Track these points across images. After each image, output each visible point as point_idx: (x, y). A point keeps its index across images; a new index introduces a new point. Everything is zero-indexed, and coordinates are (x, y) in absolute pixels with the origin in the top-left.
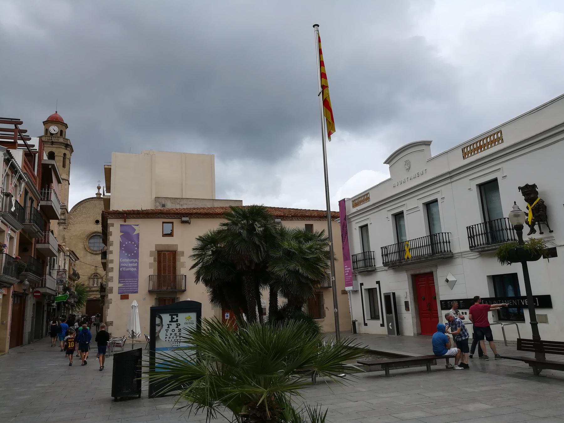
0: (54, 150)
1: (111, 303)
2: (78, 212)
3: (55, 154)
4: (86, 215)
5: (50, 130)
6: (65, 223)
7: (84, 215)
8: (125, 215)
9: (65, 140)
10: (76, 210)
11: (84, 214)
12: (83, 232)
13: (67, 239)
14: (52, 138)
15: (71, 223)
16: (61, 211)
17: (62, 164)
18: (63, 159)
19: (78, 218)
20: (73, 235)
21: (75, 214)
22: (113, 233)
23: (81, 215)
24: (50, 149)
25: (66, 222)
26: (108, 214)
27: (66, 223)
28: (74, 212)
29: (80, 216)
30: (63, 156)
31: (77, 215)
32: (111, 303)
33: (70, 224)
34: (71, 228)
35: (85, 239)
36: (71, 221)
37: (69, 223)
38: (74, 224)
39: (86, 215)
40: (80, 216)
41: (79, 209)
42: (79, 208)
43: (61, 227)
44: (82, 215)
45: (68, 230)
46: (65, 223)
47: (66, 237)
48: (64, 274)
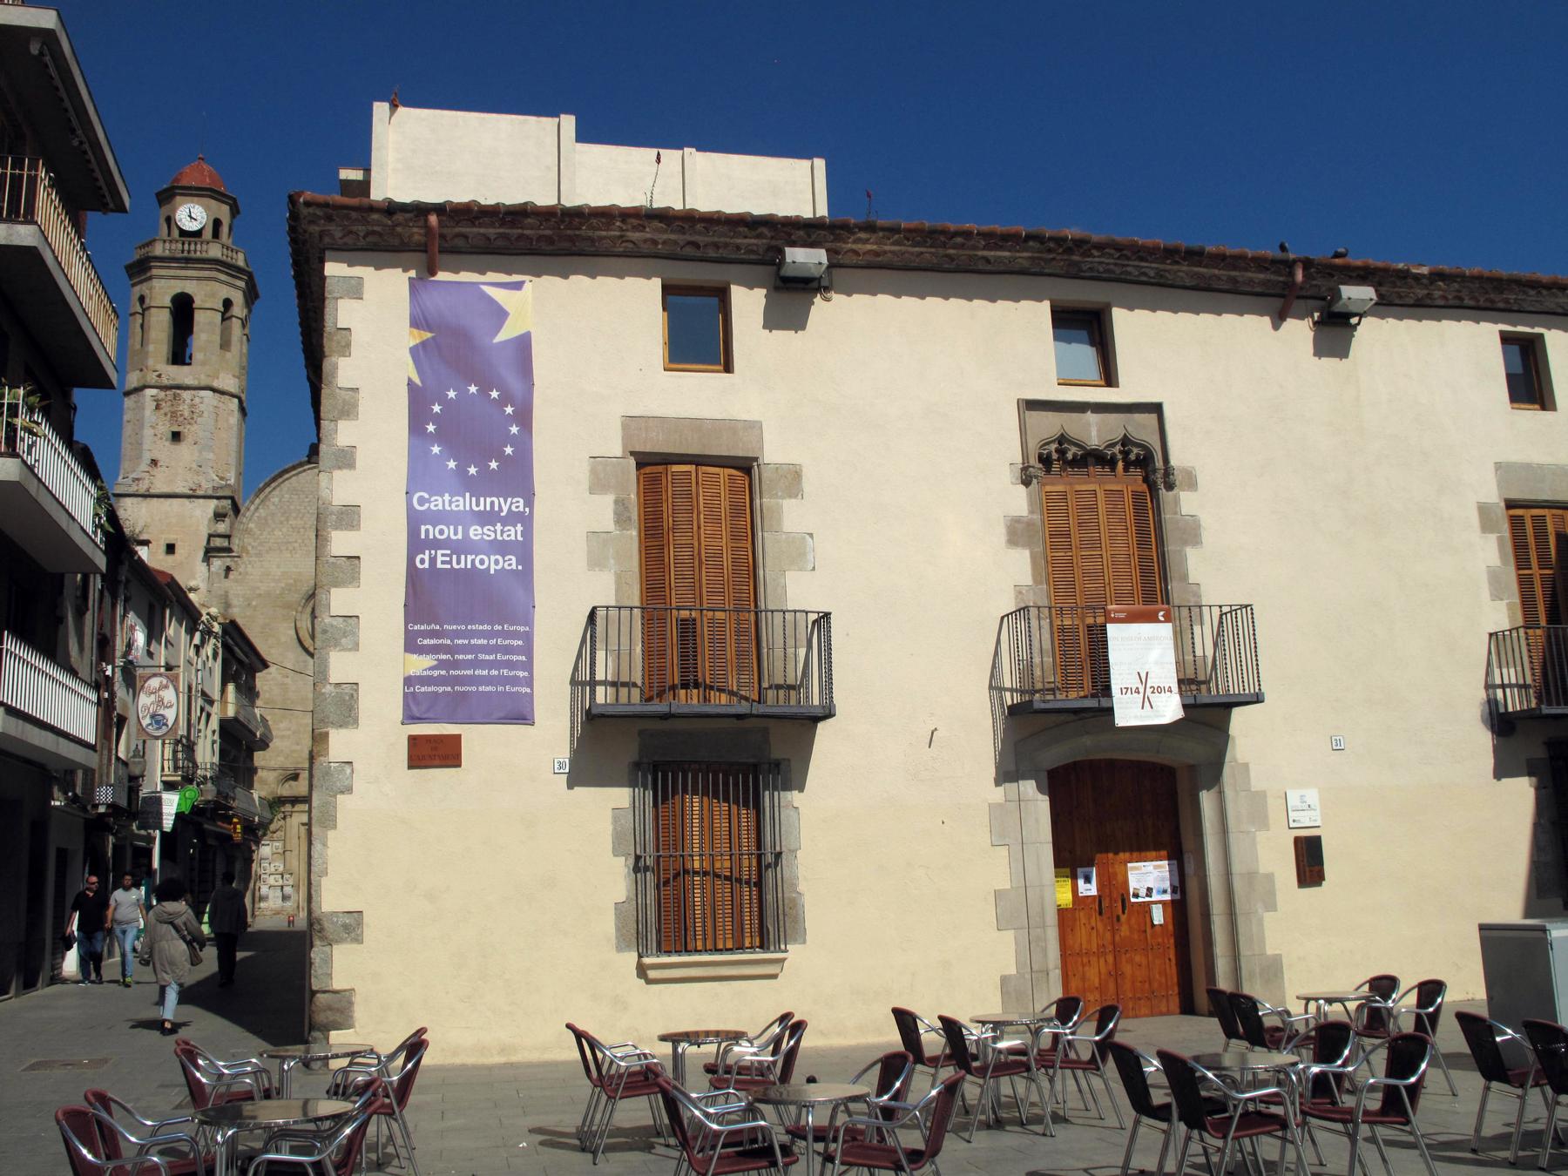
0: (189, 287)
1: (349, 790)
2: (272, 507)
3: (193, 301)
4: (301, 519)
5: (181, 220)
6: (229, 550)
7: (295, 518)
8: (433, 219)
9: (230, 252)
10: (267, 503)
11: (294, 515)
12: (292, 581)
13: (235, 607)
14: (183, 244)
15: (250, 548)
16: (217, 507)
17: (217, 338)
18: (223, 320)
19: (273, 530)
20: (258, 592)
21: (263, 515)
22: (354, 338)
23: (282, 519)
24: (179, 287)
25: (231, 546)
26: (329, 219)
27: (235, 548)
28: (261, 511)
29: (281, 523)
30: (222, 309)
31: (269, 518)
32: (349, 790)
33: (248, 553)
34: (249, 569)
35: (300, 609)
36: (251, 540)
37: (244, 549)
38: (259, 555)
39: (301, 519)
40: (281, 523)
41: (276, 500)
42: (276, 492)
43: (217, 564)
44: (287, 520)
45: (240, 574)
46: (229, 550)
47: (235, 602)
48: (166, 687)
